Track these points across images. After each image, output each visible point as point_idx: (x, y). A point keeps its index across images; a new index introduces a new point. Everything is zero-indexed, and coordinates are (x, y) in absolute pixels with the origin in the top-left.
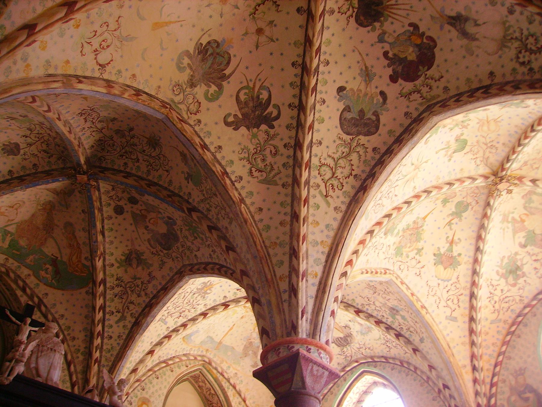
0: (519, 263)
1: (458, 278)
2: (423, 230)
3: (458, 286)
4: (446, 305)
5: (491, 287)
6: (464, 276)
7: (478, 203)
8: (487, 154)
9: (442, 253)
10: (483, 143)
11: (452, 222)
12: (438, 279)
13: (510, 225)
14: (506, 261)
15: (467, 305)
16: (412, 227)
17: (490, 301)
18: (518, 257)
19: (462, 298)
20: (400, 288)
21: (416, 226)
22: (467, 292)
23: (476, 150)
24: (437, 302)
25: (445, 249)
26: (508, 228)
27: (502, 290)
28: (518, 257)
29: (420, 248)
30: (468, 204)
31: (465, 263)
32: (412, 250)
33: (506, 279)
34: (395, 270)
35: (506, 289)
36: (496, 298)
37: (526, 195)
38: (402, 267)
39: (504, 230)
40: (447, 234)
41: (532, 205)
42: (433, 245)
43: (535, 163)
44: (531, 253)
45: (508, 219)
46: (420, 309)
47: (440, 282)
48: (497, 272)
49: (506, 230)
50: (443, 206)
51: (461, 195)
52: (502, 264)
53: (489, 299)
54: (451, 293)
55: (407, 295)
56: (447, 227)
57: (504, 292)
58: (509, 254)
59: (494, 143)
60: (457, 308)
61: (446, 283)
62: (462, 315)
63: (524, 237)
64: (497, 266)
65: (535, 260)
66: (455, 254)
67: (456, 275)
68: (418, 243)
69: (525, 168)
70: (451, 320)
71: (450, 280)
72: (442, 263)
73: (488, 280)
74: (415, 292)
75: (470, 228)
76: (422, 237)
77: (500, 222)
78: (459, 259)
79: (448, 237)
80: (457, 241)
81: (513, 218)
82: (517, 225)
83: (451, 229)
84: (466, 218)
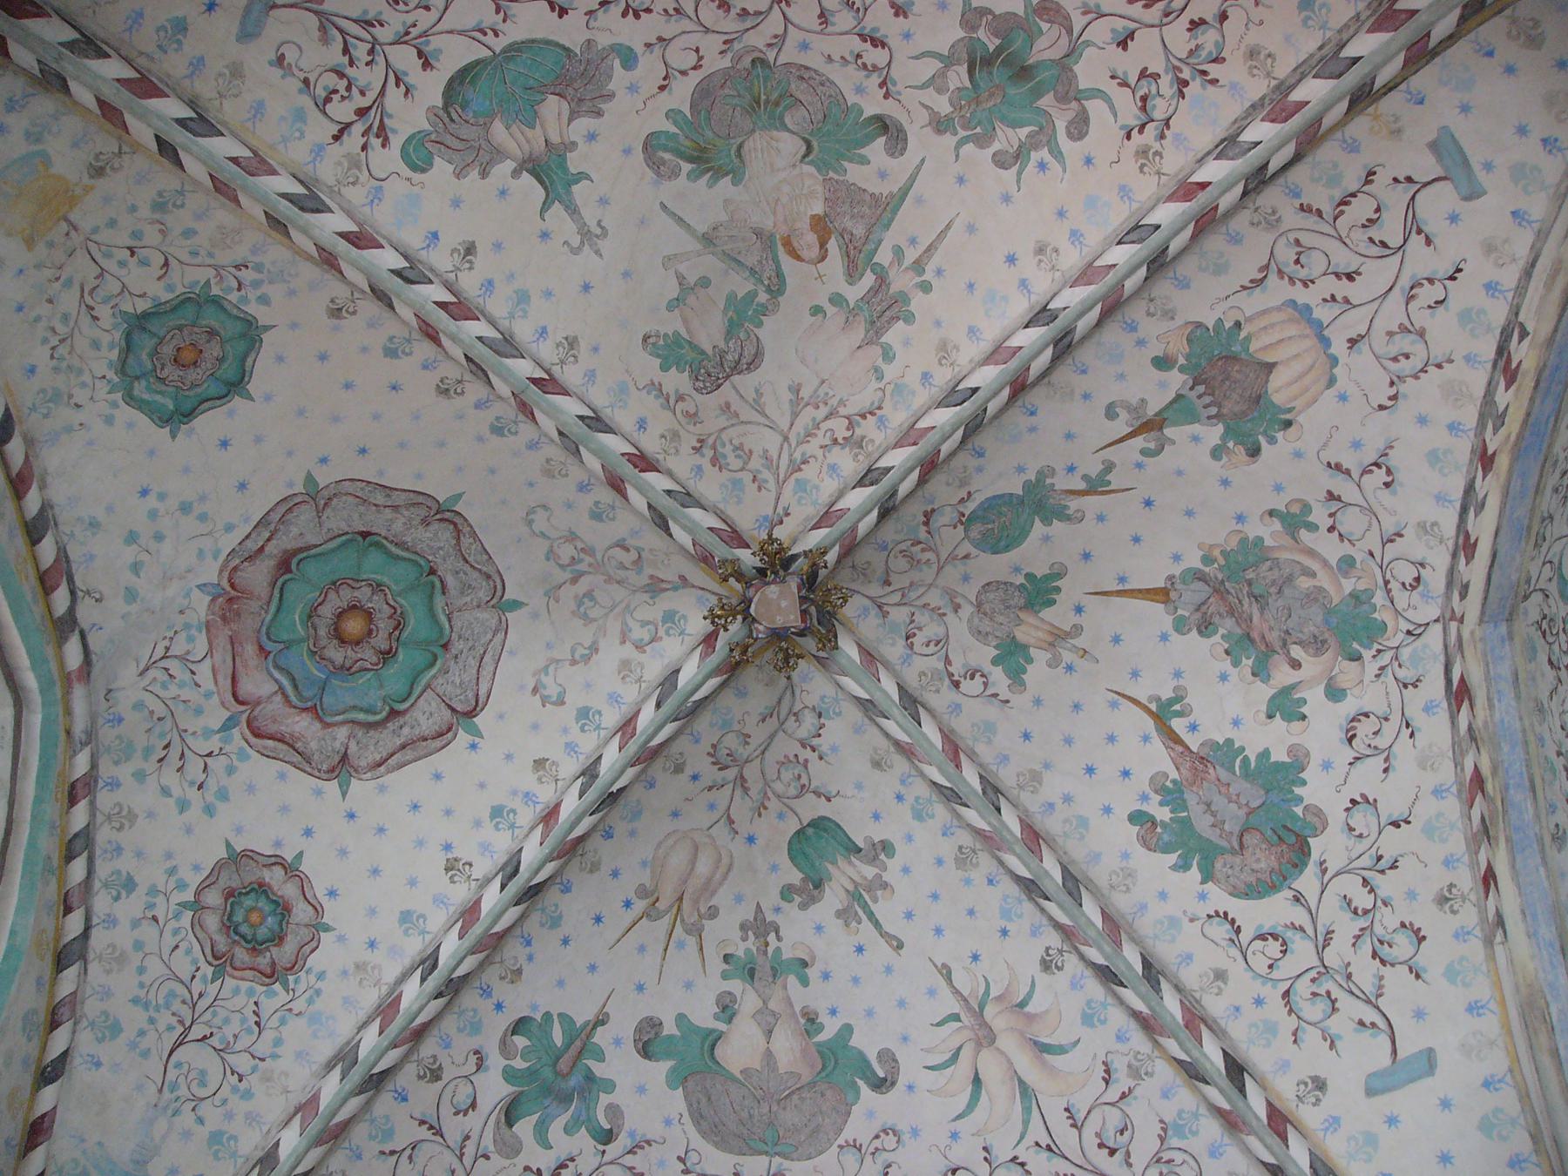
0: (959, 77)
1: (1258, 283)
2: (1207, 559)
3: (1286, 254)
4: (1416, 241)
5: (1159, 110)
6: (1220, 269)
7: (928, 515)
8: (759, 735)
9: (1220, 429)
10: (746, 790)
11: (1082, 486)
12: (1334, 361)
13: (884, 256)
14: (1007, 138)
15: (1328, 152)
16: (1230, 623)
17: (1218, 60)
18: (943, 106)
19: (1323, 199)
20: (1494, 556)
21: (1215, 605)
22: (1271, 197)
23: (787, 775)
24: (1437, 292)
25: (1196, 428)
26: (898, 252)
27: (1123, 44)
28: (943, 106)
29: (1277, 525)
30: (966, 521)
31: (1170, 315)
32: (1311, 553)
33: (1064, 65)
34: (1433, 611)
35: (1101, 32)
36: (1178, 37)
37: (736, 369)
38: (1408, 574)
39: (918, 266)
40: (1139, 466)
41: (741, 285)
42: (1225, 483)
43: (622, 567)
44: (875, 79)
45: (875, 291)
46: (1526, 382)
47: (1339, 347)
48: (1078, 130)
49: (911, 255)
50: (1060, 575)
51: (966, 578)
52: (1032, 144)
53: (1214, 70)
54: (1344, 259)
55: (1506, 494)
56: (1115, 480)
57: (1121, 24)
58: (969, 148)
59: (710, 773)
60: (1382, 178)
61: (1323, 313)
62: (1397, 133)
63: (864, 161)
64: (1058, 154)
65: (878, 43)
66: (1176, 380)
67: (1252, 303)
68: (1268, 542)
69: (670, 575)
70: (1466, 163)
71: (1292, 303)
72: (1258, 399)
73: (1143, 152)
74: (1463, 448)
75: (1033, 429)
76: (1233, 543)
77: (909, 318)
78: (1179, 348)
79: (1144, 452)
80: (1123, 415)
81: (852, 274)
82: (859, 231)
83: (1109, 467)
84: (1021, 469)
